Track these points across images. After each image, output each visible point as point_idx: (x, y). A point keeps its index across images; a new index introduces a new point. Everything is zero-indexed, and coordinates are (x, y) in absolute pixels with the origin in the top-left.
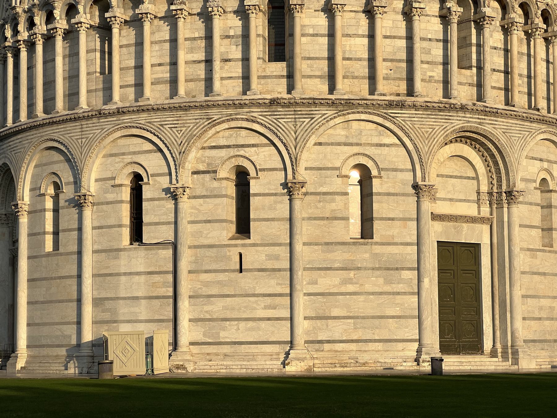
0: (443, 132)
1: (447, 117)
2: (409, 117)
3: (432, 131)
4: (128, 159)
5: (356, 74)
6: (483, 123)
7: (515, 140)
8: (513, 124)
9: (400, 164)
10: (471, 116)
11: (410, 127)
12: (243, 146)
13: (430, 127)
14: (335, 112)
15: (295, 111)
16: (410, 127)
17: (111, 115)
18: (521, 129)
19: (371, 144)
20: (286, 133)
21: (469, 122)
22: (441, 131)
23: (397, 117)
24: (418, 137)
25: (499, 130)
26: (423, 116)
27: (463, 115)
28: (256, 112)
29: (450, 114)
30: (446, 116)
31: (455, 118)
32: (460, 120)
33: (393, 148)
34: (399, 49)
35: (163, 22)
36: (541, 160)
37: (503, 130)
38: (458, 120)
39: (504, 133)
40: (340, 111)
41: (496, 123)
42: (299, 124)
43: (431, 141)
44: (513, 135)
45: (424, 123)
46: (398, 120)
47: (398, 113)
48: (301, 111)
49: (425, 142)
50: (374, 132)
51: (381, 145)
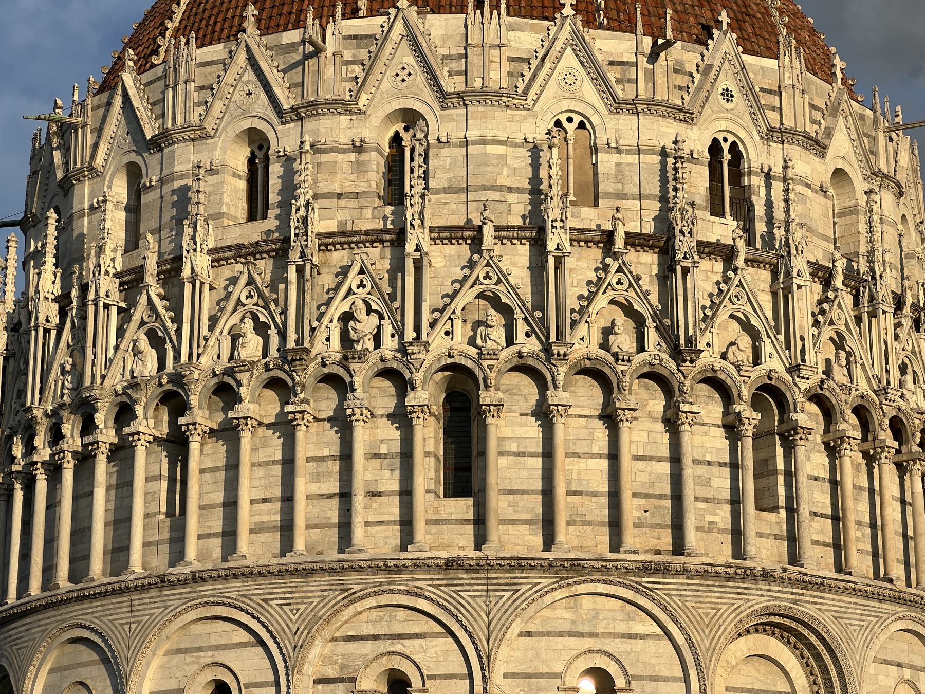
0: (734, 615)
1: (739, 590)
2: (677, 590)
3: (716, 614)
4: (207, 657)
5: (589, 518)
6: (800, 601)
7: (855, 631)
8: (850, 603)
9: (663, 668)
10: (780, 589)
11: (678, 605)
12: (400, 636)
13: (713, 606)
14: (554, 580)
15: (487, 578)
16: (678, 605)
17: (181, 583)
19: (614, 634)
20: (472, 615)
21: (776, 598)
22: (731, 613)
23: (657, 589)
24: (692, 622)
25: (827, 613)
26: (701, 588)
27: (767, 587)
28: (423, 581)
29: (745, 585)
30: (738, 588)
31: (754, 592)
32: (762, 596)
33: (651, 641)
34: (659, 477)
35: (272, 431)
37: (835, 614)
38: (758, 595)
39: (836, 618)
40: (562, 579)
41: (822, 601)
43: (715, 630)
45: (701, 599)
46: (658, 595)
47: (659, 583)
48: (497, 578)
50: (618, 614)
51: (630, 636)
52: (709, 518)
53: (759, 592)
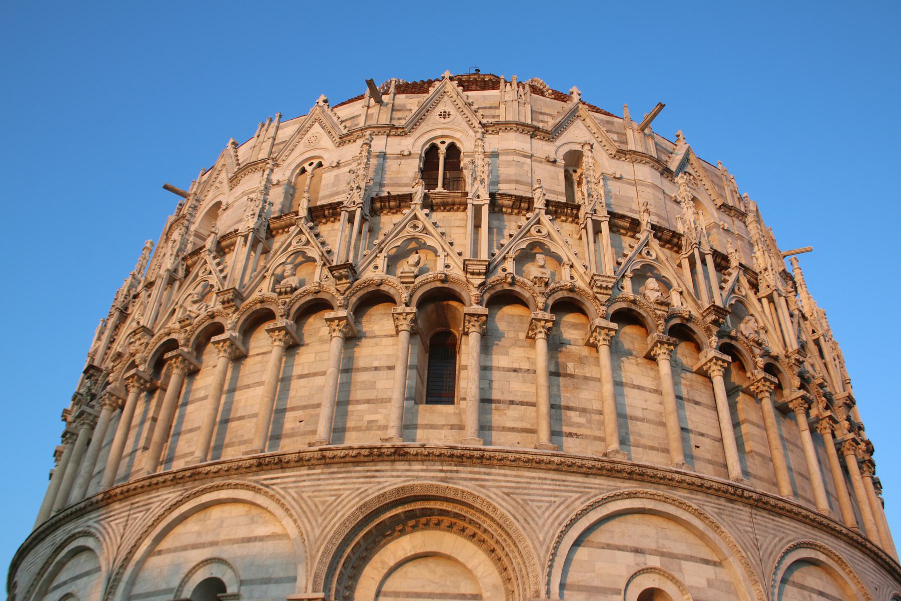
1: (368, 474)
2: (295, 482)
3: (335, 500)
6: (451, 478)
7: (539, 507)
8: (534, 478)
10: (424, 467)
13: (333, 493)
16: (293, 498)
18: (557, 488)
21: (418, 477)
22: (354, 498)
23: (273, 484)
24: (304, 512)
25: (494, 490)
27: (407, 467)
29: (378, 468)
31: (388, 474)
32: (398, 477)
34: (321, 388)
36: (637, 551)
37: (506, 490)
39: (508, 494)
40: (187, 490)
41: (486, 477)
42: (130, 522)
43: (330, 517)
44: (532, 497)
45: (320, 488)
46: (273, 490)
47: (278, 478)
49: (317, 521)
52: (368, 417)
53: (395, 473)
